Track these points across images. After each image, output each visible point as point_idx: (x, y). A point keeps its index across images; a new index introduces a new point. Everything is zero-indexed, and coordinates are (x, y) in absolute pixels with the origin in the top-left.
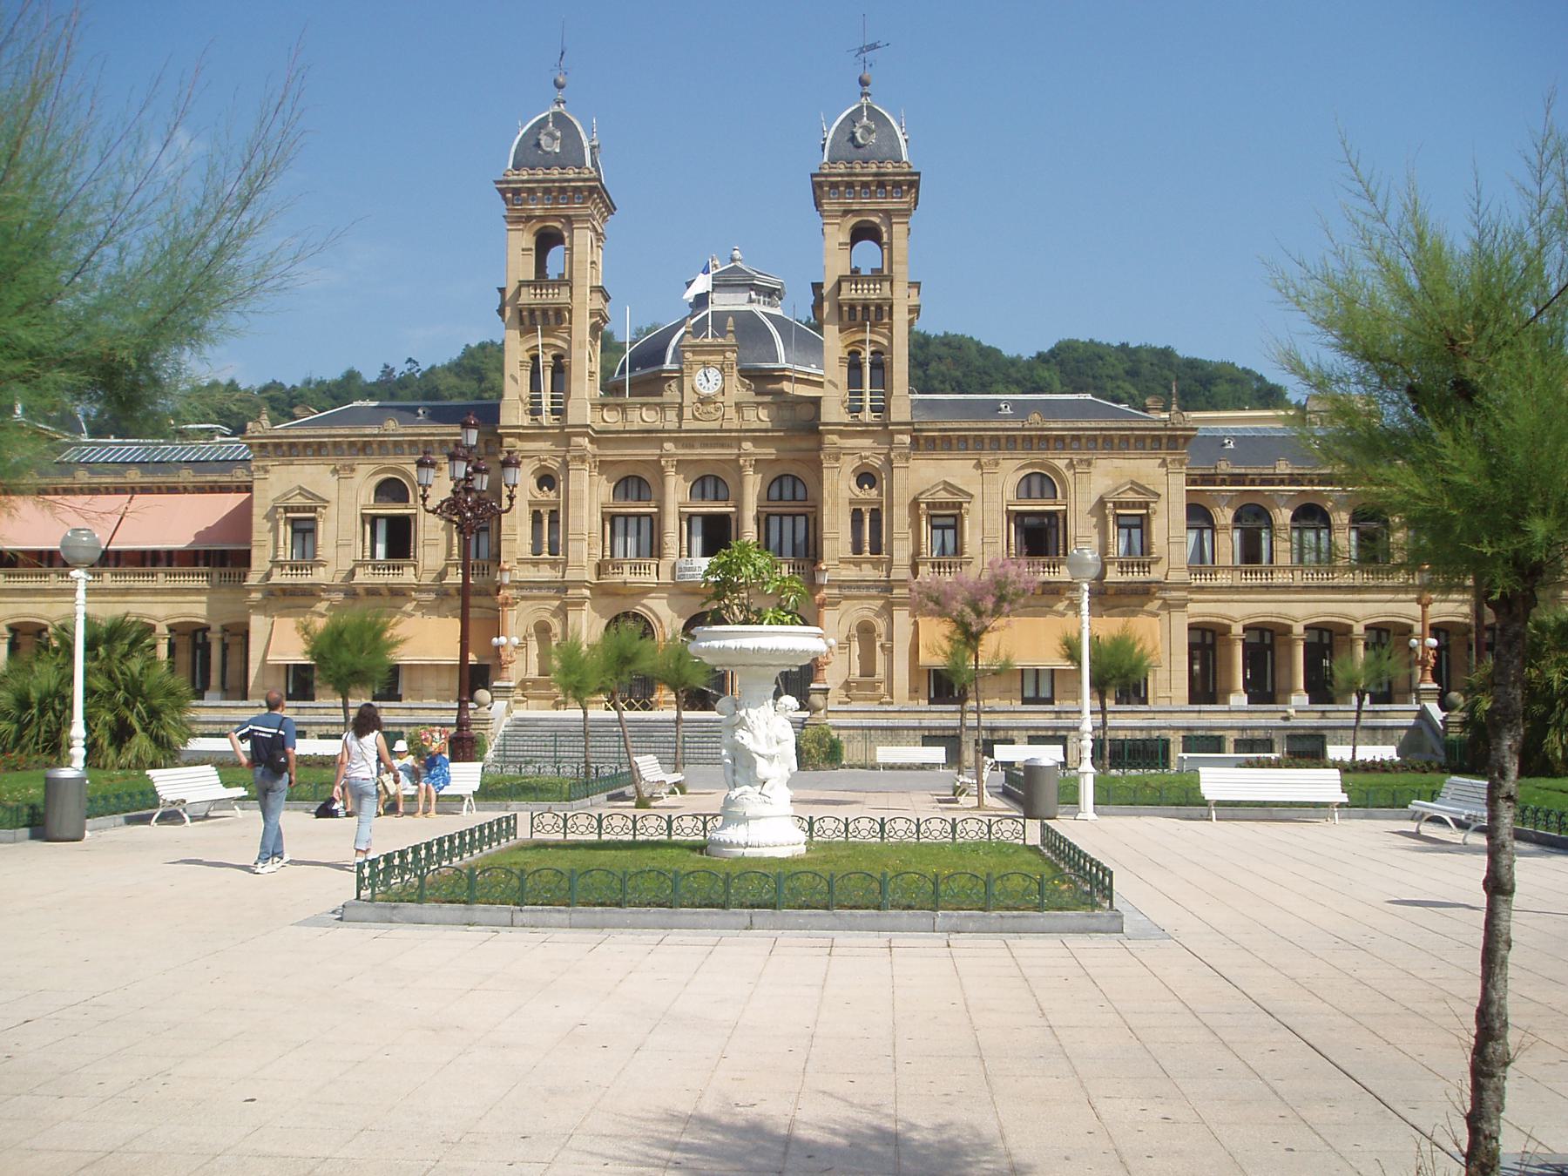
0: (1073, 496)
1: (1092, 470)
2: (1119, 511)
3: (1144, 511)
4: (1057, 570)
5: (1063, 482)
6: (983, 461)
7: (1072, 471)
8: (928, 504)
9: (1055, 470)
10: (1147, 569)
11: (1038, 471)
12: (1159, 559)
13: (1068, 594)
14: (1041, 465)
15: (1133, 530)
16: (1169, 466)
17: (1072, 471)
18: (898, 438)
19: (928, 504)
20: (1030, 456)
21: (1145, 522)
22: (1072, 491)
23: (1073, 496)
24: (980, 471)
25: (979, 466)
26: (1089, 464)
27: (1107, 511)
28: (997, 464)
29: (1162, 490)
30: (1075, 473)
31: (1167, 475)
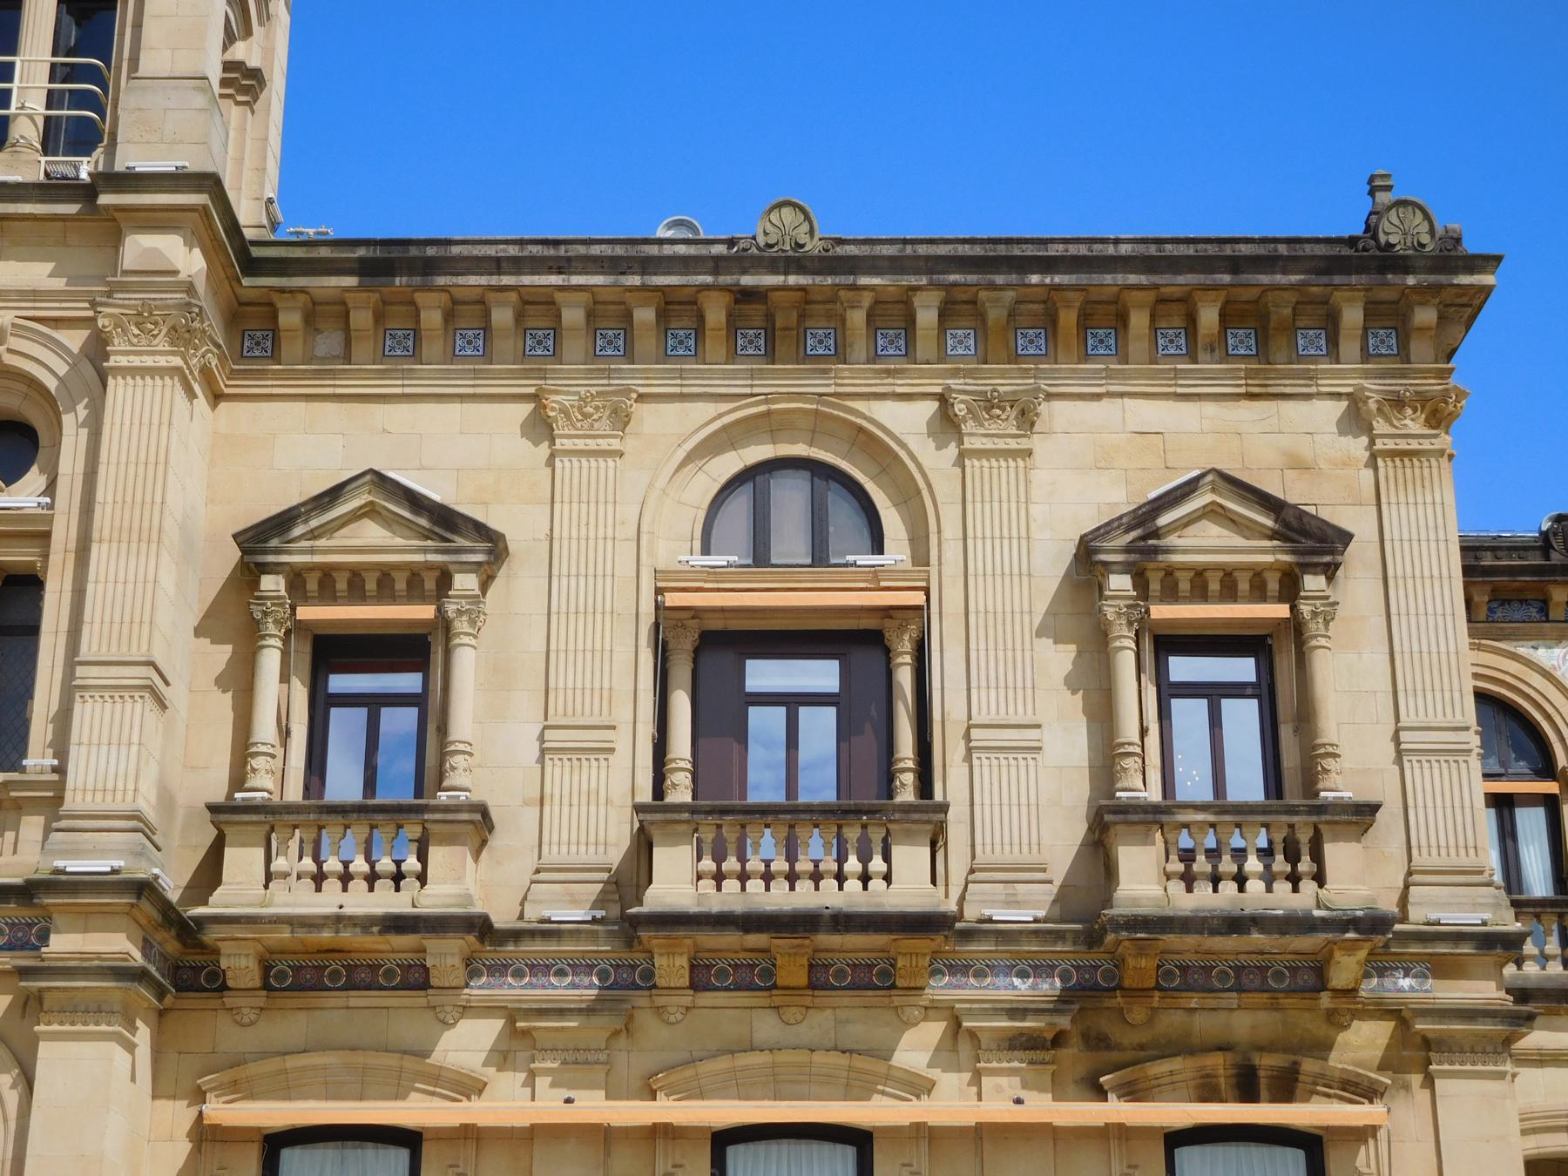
0: (952, 552)
1: (1035, 442)
2: (1161, 612)
3: (1282, 611)
4: (877, 864)
5: (911, 498)
6: (554, 401)
7: (952, 450)
8: (297, 579)
9: (868, 443)
10: (1305, 865)
11: (800, 450)
12: (1363, 814)
13: (941, 989)
14: (819, 425)
15: (1227, 705)
16: (1380, 426)
17: (952, 450)
18: (140, 248)
19: (297, 579)
20: (764, 386)
21: (1285, 664)
22: (951, 529)
23: (952, 552)
24: (544, 450)
25: (540, 427)
26: (1027, 419)
27: (1110, 613)
28: (621, 420)
29: (1355, 519)
30: (962, 456)
31: (1372, 462)
